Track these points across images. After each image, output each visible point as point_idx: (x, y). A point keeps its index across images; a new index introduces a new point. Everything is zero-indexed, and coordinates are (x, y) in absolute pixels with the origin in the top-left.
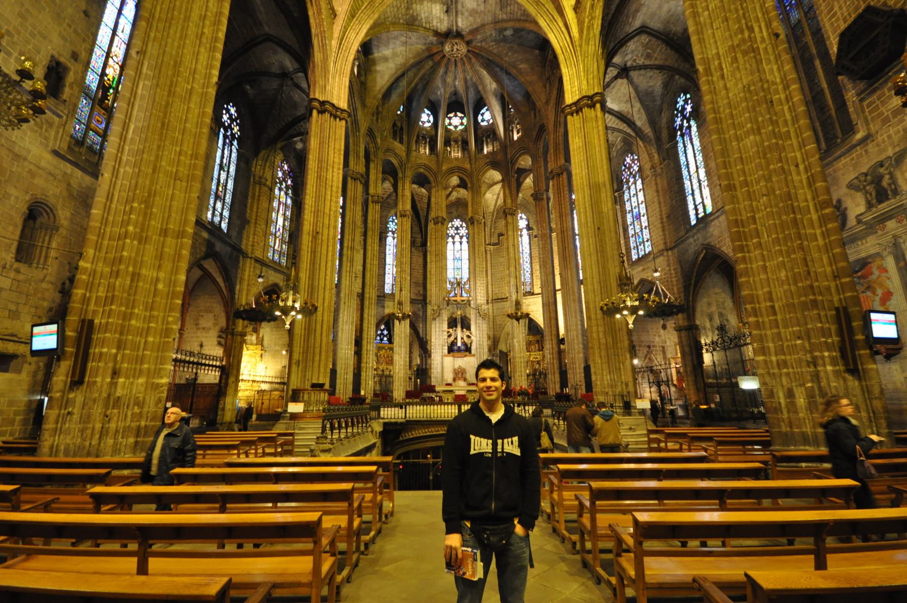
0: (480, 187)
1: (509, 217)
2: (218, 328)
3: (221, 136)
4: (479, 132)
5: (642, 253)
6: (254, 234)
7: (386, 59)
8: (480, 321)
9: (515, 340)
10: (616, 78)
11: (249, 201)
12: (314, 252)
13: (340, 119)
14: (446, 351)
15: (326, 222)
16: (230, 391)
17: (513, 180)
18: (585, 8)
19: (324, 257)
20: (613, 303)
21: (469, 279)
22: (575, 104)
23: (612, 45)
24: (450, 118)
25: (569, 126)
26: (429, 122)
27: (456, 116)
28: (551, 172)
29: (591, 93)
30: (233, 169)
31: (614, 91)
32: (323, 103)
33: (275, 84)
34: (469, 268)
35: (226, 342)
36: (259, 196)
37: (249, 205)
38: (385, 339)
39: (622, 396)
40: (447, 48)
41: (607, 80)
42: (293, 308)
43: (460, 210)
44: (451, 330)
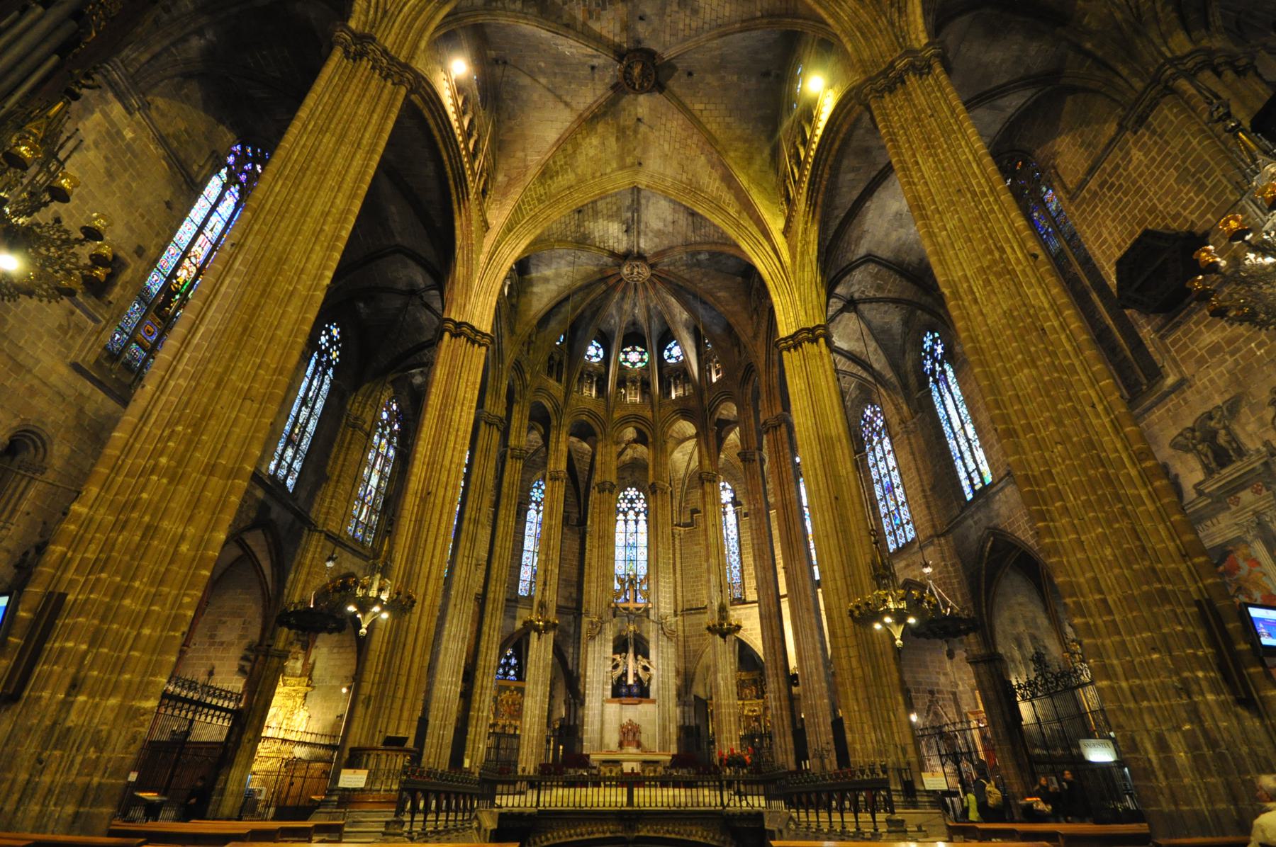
0: (665, 442)
1: (707, 484)
2: (245, 642)
3: (313, 361)
4: (665, 371)
5: (902, 541)
6: (332, 497)
7: (546, 280)
8: (664, 642)
9: (720, 675)
10: (841, 311)
11: (335, 450)
12: (419, 521)
13: (480, 345)
14: (609, 693)
15: (444, 479)
16: (241, 759)
17: (712, 435)
18: (797, 232)
19: (433, 530)
20: (867, 604)
21: (647, 577)
22: (792, 337)
23: (833, 274)
24: (626, 353)
25: (786, 363)
26: (597, 356)
27: (634, 350)
28: (765, 423)
29: (811, 325)
30: (319, 405)
31: (840, 328)
32: (459, 325)
33: (398, 302)
34: (648, 560)
35: (252, 669)
36: (350, 443)
37: (332, 456)
38: (512, 672)
39: (899, 770)
40: (625, 271)
41: (830, 313)
42: (377, 600)
43: (637, 474)
44: (618, 657)
